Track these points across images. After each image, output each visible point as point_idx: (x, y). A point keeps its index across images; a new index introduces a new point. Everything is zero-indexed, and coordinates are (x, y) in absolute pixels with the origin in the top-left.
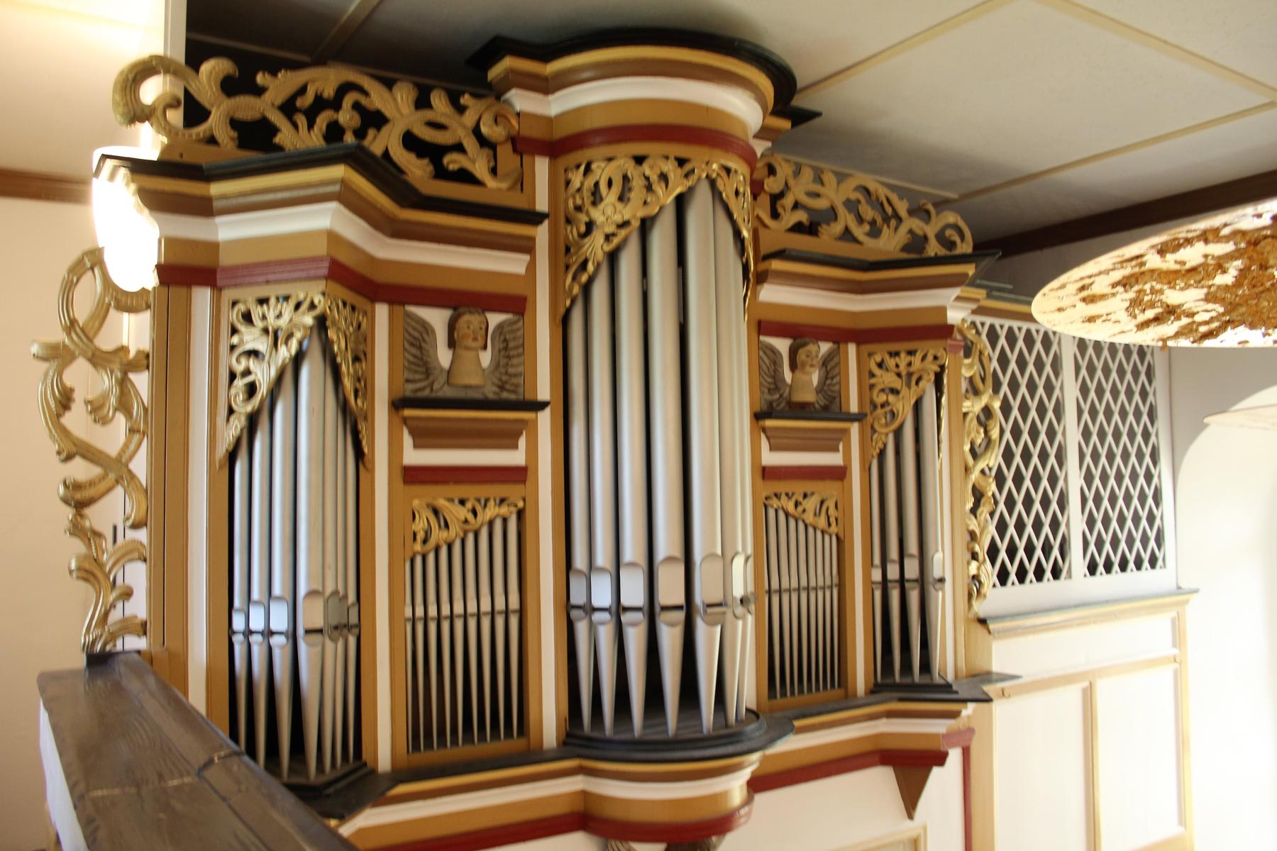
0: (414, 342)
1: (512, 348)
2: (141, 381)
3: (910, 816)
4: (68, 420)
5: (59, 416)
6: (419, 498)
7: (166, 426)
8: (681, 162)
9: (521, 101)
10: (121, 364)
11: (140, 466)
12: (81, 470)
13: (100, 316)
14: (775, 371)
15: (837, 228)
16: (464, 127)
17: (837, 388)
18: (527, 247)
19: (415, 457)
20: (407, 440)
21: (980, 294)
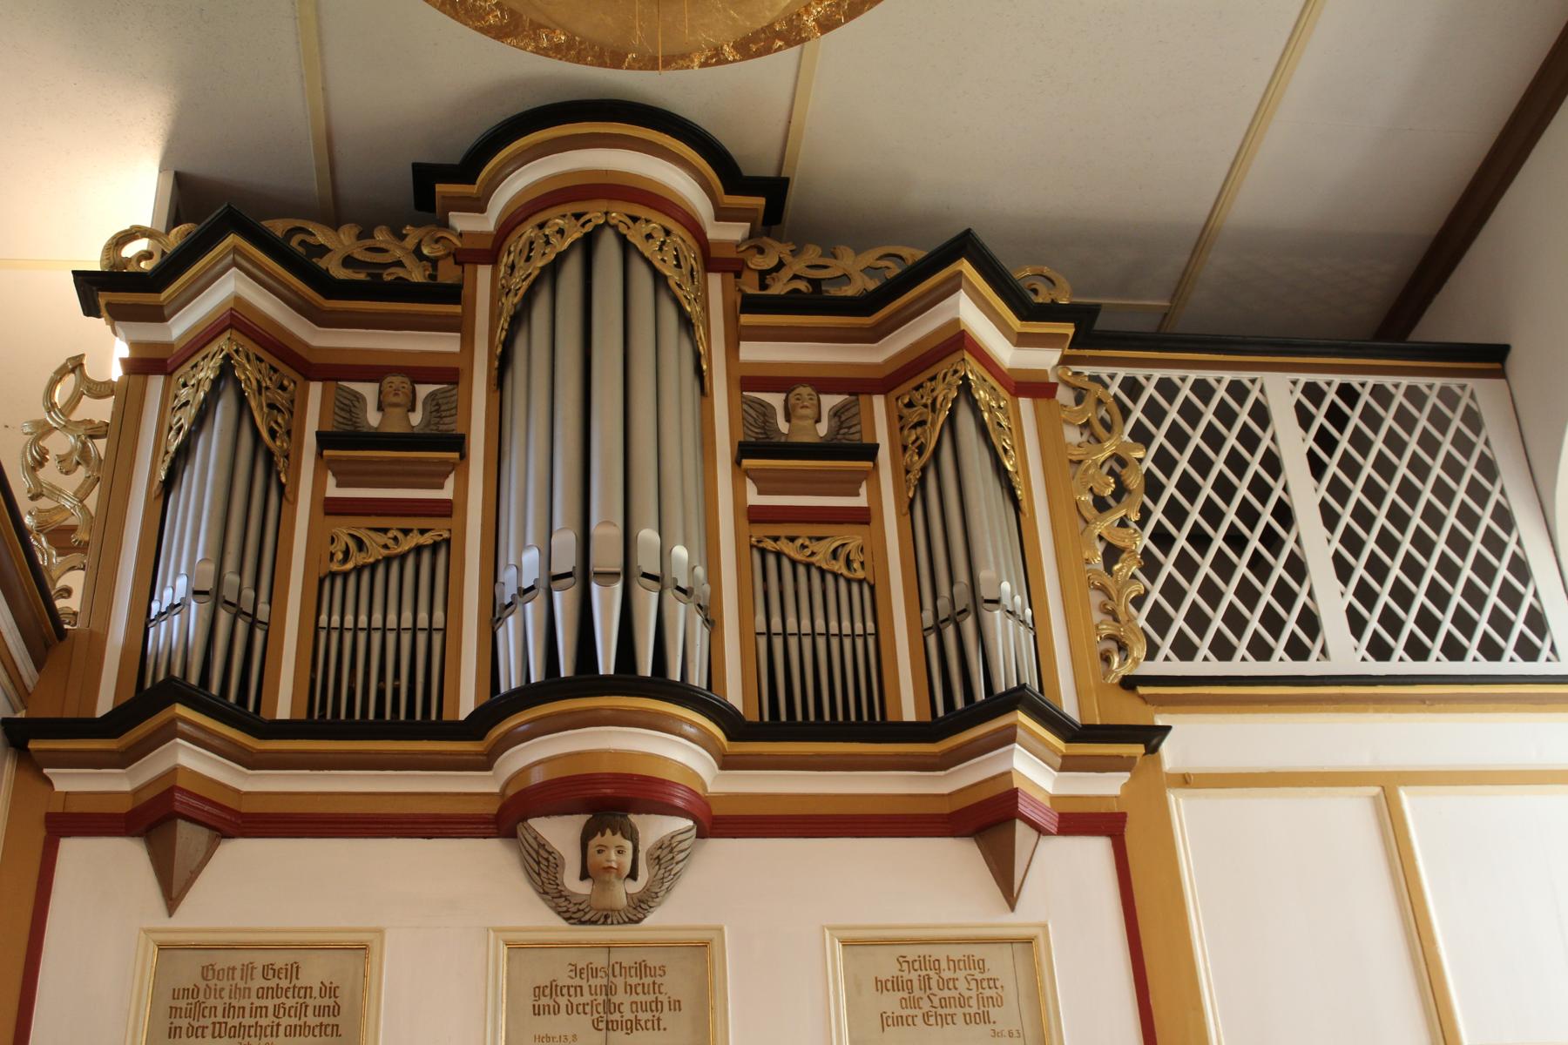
3: (1012, 908)
4: (42, 474)
5: (34, 469)
6: (343, 529)
8: (577, 216)
9: (462, 222)
14: (765, 422)
16: (403, 248)
17: (857, 436)
18: (462, 326)
19: (333, 491)
20: (331, 481)
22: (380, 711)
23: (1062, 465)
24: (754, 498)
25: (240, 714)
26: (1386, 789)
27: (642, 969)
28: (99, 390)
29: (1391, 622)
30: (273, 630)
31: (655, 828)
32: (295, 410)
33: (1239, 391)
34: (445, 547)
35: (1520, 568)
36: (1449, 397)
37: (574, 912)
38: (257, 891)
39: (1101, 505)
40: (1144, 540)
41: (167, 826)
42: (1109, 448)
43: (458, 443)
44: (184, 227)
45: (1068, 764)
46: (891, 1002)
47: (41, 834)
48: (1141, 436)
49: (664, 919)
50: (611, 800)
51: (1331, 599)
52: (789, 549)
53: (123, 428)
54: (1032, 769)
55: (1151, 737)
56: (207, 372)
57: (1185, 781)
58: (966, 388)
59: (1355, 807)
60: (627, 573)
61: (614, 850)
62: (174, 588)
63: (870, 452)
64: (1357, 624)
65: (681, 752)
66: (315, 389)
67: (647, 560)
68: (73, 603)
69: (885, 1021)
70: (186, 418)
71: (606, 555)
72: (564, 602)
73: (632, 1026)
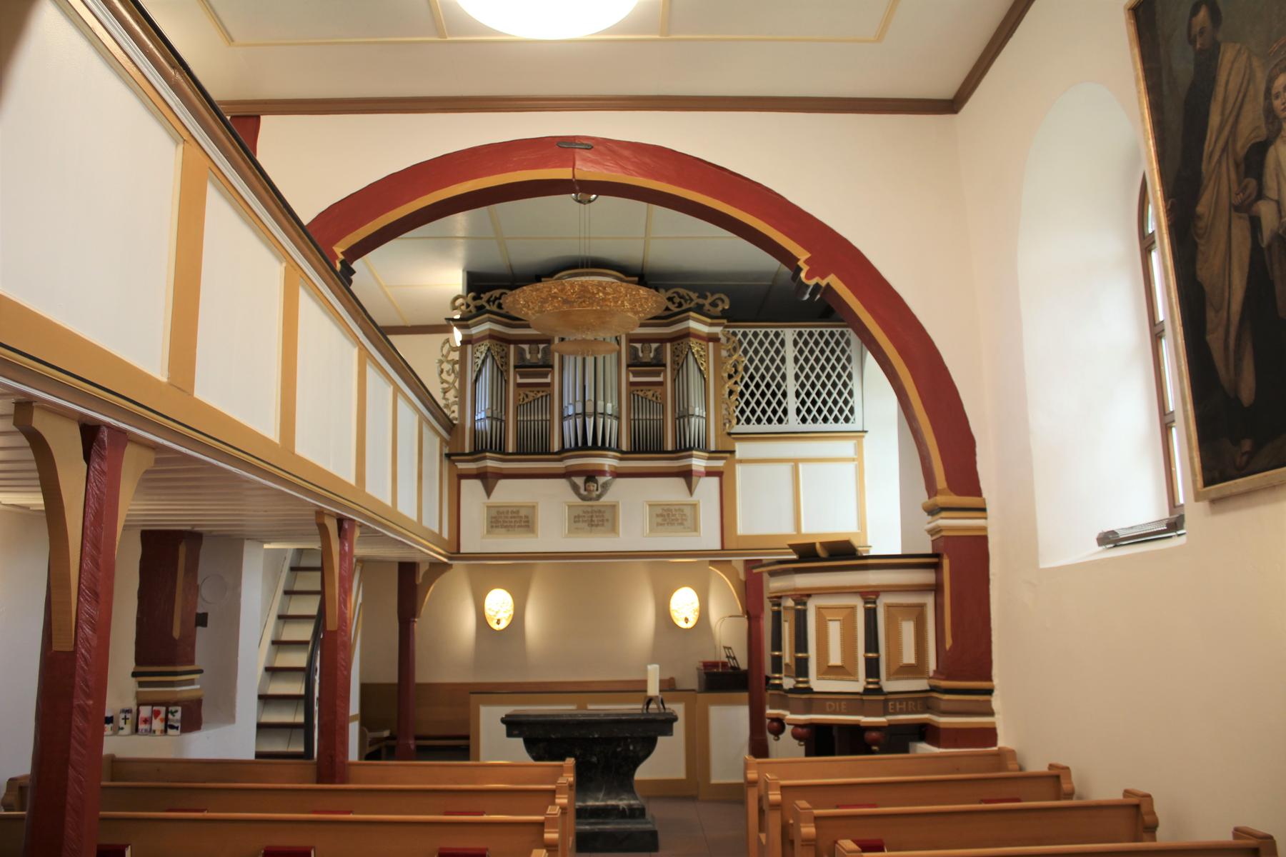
0: (520, 354)
1: (547, 352)
2: (457, 367)
6: (522, 391)
7: (462, 375)
10: (455, 362)
11: (457, 384)
12: (445, 385)
21: (725, 321)
22: (534, 445)
23: (719, 362)
24: (632, 379)
25: (500, 449)
26: (796, 462)
28: (454, 349)
29: (809, 411)
30: (506, 422)
31: (602, 480)
32: (507, 356)
33: (777, 335)
34: (551, 395)
35: (851, 394)
36: (842, 334)
37: (583, 498)
38: (508, 492)
39: (730, 377)
40: (741, 387)
41: (488, 479)
42: (735, 357)
44: (471, 295)
45: (709, 459)
46: (660, 520)
47: (456, 479)
48: (745, 352)
49: (606, 499)
50: (591, 475)
51: (792, 403)
52: (641, 394)
53: (462, 361)
54: (698, 463)
55: (733, 452)
56: (483, 349)
57: (741, 461)
58: (690, 348)
59: (786, 469)
60: (595, 413)
61: (592, 486)
63: (665, 365)
64: (798, 411)
66: (512, 347)
67: (600, 410)
68: (456, 415)
69: (659, 524)
70: (480, 362)
71: (590, 408)
72: (579, 421)
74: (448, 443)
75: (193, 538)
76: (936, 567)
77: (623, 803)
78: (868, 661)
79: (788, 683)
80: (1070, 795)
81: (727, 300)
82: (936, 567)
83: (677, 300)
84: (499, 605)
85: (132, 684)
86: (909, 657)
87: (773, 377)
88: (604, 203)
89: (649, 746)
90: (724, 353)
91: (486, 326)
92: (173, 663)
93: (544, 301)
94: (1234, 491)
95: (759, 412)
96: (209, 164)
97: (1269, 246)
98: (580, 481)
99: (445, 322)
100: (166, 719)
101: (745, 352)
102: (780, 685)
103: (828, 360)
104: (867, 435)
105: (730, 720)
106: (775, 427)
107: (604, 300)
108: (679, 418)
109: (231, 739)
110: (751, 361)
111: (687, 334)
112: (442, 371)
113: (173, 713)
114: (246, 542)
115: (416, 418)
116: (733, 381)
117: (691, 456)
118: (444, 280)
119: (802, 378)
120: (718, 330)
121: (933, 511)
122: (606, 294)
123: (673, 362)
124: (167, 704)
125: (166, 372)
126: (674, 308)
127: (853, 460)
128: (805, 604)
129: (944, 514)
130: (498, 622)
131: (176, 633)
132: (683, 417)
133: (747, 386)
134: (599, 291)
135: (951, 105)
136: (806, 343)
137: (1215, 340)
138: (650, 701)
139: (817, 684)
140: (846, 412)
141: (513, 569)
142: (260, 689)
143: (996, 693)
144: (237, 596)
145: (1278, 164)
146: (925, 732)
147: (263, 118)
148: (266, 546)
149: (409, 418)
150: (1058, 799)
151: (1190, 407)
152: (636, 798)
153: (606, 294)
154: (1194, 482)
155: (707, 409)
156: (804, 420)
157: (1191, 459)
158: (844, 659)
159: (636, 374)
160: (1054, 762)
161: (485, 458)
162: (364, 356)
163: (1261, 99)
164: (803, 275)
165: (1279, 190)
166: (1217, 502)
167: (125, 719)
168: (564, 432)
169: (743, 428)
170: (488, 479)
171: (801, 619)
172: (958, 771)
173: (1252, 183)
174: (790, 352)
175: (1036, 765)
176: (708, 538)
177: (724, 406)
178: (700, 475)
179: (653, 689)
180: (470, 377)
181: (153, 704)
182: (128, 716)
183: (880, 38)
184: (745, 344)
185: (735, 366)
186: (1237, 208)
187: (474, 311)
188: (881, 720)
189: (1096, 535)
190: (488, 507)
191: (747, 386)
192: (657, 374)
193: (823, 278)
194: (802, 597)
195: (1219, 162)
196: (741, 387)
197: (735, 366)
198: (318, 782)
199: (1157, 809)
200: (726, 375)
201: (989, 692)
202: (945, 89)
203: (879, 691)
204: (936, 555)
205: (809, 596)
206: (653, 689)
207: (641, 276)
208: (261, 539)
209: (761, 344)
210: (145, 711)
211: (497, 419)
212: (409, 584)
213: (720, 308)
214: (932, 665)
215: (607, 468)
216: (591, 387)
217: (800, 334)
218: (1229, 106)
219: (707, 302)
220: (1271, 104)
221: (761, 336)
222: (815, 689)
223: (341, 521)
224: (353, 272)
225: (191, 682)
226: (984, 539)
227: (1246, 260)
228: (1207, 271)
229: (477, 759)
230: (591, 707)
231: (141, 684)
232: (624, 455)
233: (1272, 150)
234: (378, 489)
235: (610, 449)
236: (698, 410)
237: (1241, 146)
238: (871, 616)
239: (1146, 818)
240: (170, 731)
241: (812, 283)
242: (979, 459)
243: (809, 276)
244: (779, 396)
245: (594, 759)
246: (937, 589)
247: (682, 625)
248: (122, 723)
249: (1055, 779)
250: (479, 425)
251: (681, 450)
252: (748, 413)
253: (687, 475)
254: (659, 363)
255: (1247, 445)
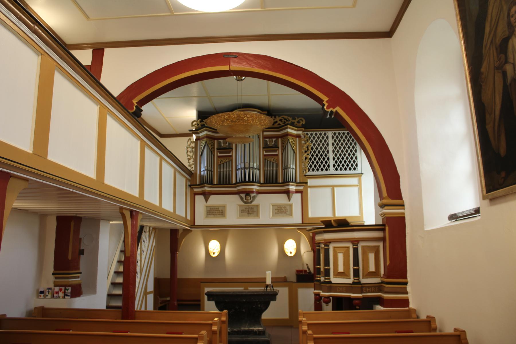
0: (219, 144)
2: (194, 149)
6: (220, 159)
7: (196, 153)
10: (193, 148)
11: (194, 157)
12: (189, 157)
13: (190, 144)
15: (277, 123)
19: (219, 155)
21: (303, 129)
22: (225, 181)
23: (301, 146)
24: (265, 153)
25: (211, 183)
26: (333, 187)
27: (252, 208)
28: (192, 142)
29: (339, 166)
30: (214, 172)
31: (252, 195)
32: (214, 145)
33: (325, 134)
34: (232, 160)
35: (356, 158)
37: (245, 203)
38: (215, 200)
39: (306, 152)
40: (310, 156)
41: (206, 195)
42: (308, 143)
43: (232, 149)
44: (199, 120)
45: (297, 186)
46: (276, 211)
47: (193, 195)
48: (312, 141)
49: (254, 203)
50: (248, 193)
51: (331, 162)
52: (269, 159)
53: (196, 147)
54: (292, 188)
55: (307, 183)
56: (204, 142)
57: (310, 187)
58: (288, 140)
59: (329, 190)
60: (249, 168)
61: (249, 198)
62: (203, 169)
63: (278, 148)
64: (334, 166)
65: (255, 188)
66: (216, 141)
67: (251, 166)
68: (193, 169)
70: (203, 147)
71: (247, 166)
72: (243, 171)
73: (251, 214)
74: (190, 181)
75: (78, 219)
76: (383, 230)
77: (256, 329)
78: (354, 270)
79: (322, 279)
80: (435, 330)
81: (304, 120)
82: (383, 230)
83: (283, 120)
84: (214, 247)
85: (52, 278)
86: (372, 269)
87: (323, 152)
88: (248, 80)
89: (266, 305)
90: (303, 142)
91: (205, 133)
92: (68, 270)
93: (223, 121)
94: (498, 195)
95: (318, 166)
96: (55, 64)
97: (510, 84)
98: (243, 195)
99: (189, 132)
100: (65, 292)
101: (312, 141)
102: (320, 280)
103: (346, 144)
104: (363, 175)
105: (307, 295)
106: (324, 172)
107: (248, 120)
108: (284, 169)
109: (96, 300)
110: (314, 145)
111: (287, 134)
112: (188, 151)
113: (67, 290)
114: (101, 221)
115: (173, 170)
116: (307, 153)
117: (289, 185)
118: (190, 115)
119: (336, 152)
120: (300, 132)
121: (382, 206)
122: (248, 118)
123: (282, 146)
124: (65, 286)
125: (32, 149)
126: (282, 124)
127: (357, 186)
128: (328, 246)
129: (386, 207)
130: (214, 253)
131: (70, 258)
132: (286, 169)
133: (313, 156)
134: (245, 117)
135: (389, 34)
136: (337, 137)
137: (489, 127)
138: (267, 286)
139: (334, 280)
140: (354, 166)
141: (220, 232)
142: (112, 280)
143: (409, 284)
144: (97, 242)
145: (513, 46)
146: (380, 301)
147: (105, 50)
148: (111, 223)
149: (168, 170)
150: (430, 332)
151: (480, 158)
152: (261, 327)
153: (248, 118)
154: (482, 191)
155: (296, 166)
156: (336, 169)
157: (481, 181)
158: (344, 269)
159: (266, 151)
160: (428, 315)
161: (204, 187)
162: (143, 145)
163: (506, 18)
164: (325, 107)
165: (514, 59)
166: (492, 200)
167: (49, 292)
168: (237, 175)
169: (311, 173)
170: (206, 195)
171: (327, 252)
172: (390, 318)
173: (503, 56)
174: (330, 141)
175: (423, 317)
176: (297, 218)
177: (303, 164)
178: (293, 193)
179: (269, 282)
180: (199, 154)
181: (60, 286)
182: (50, 291)
183: (354, 5)
184: (312, 138)
185: (307, 147)
186: (497, 68)
187: (200, 127)
188: (360, 295)
189: (448, 216)
190: (206, 206)
191: (313, 156)
192: (275, 151)
193: (334, 108)
194: (327, 243)
195: (489, 48)
196: (310, 156)
197: (307, 147)
198: (122, 319)
199: (468, 337)
200: (304, 151)
201: (406, 284)
202: (386, 27)
203: (359, 283)
204: (383, 225)
205: (330, 242)
206: (269, 282)
207: (268, 111)
208: (108, 220)
209: (318, 138)
210: (57, 289)
211: (210, 171)
212: (174, 239)
213: (301, 123)
214: (382, 272)
215: (254, 190)
216: (248, 157)
217: (335, 134)
218: (493, 22)
219: (296, 121)
220: (510, 20)
221: (318, 135)
222: (333, 282)
223: (131, 212)
224: (142, 111)
225: (78, 277)
226: (404, 218)
227: (501, 91)
228: (486, 97)
229: (204, 310)
230: (250, 289)
231: (56, 278)
232: (261, 185)
233: (510, 41)
234: (151, 197)
235: (256, 182)
236: (292, 166)
237: (498, 41)
238: (356, 251)
239: (463, 341)
240: (66, 297)
241: (329, 110)
242: (401, 184)
243: (328, 108)
244: (326, 159)
245: (244, 310)
246: (383, 239)
247: (289, 255)
248: (47, 294)
249: (429, 322)
250: (203, 173)
251: (285, 182)
252: (313, 167)
253: (288, 193)
254: (275, 147)
255: (503, 174)
